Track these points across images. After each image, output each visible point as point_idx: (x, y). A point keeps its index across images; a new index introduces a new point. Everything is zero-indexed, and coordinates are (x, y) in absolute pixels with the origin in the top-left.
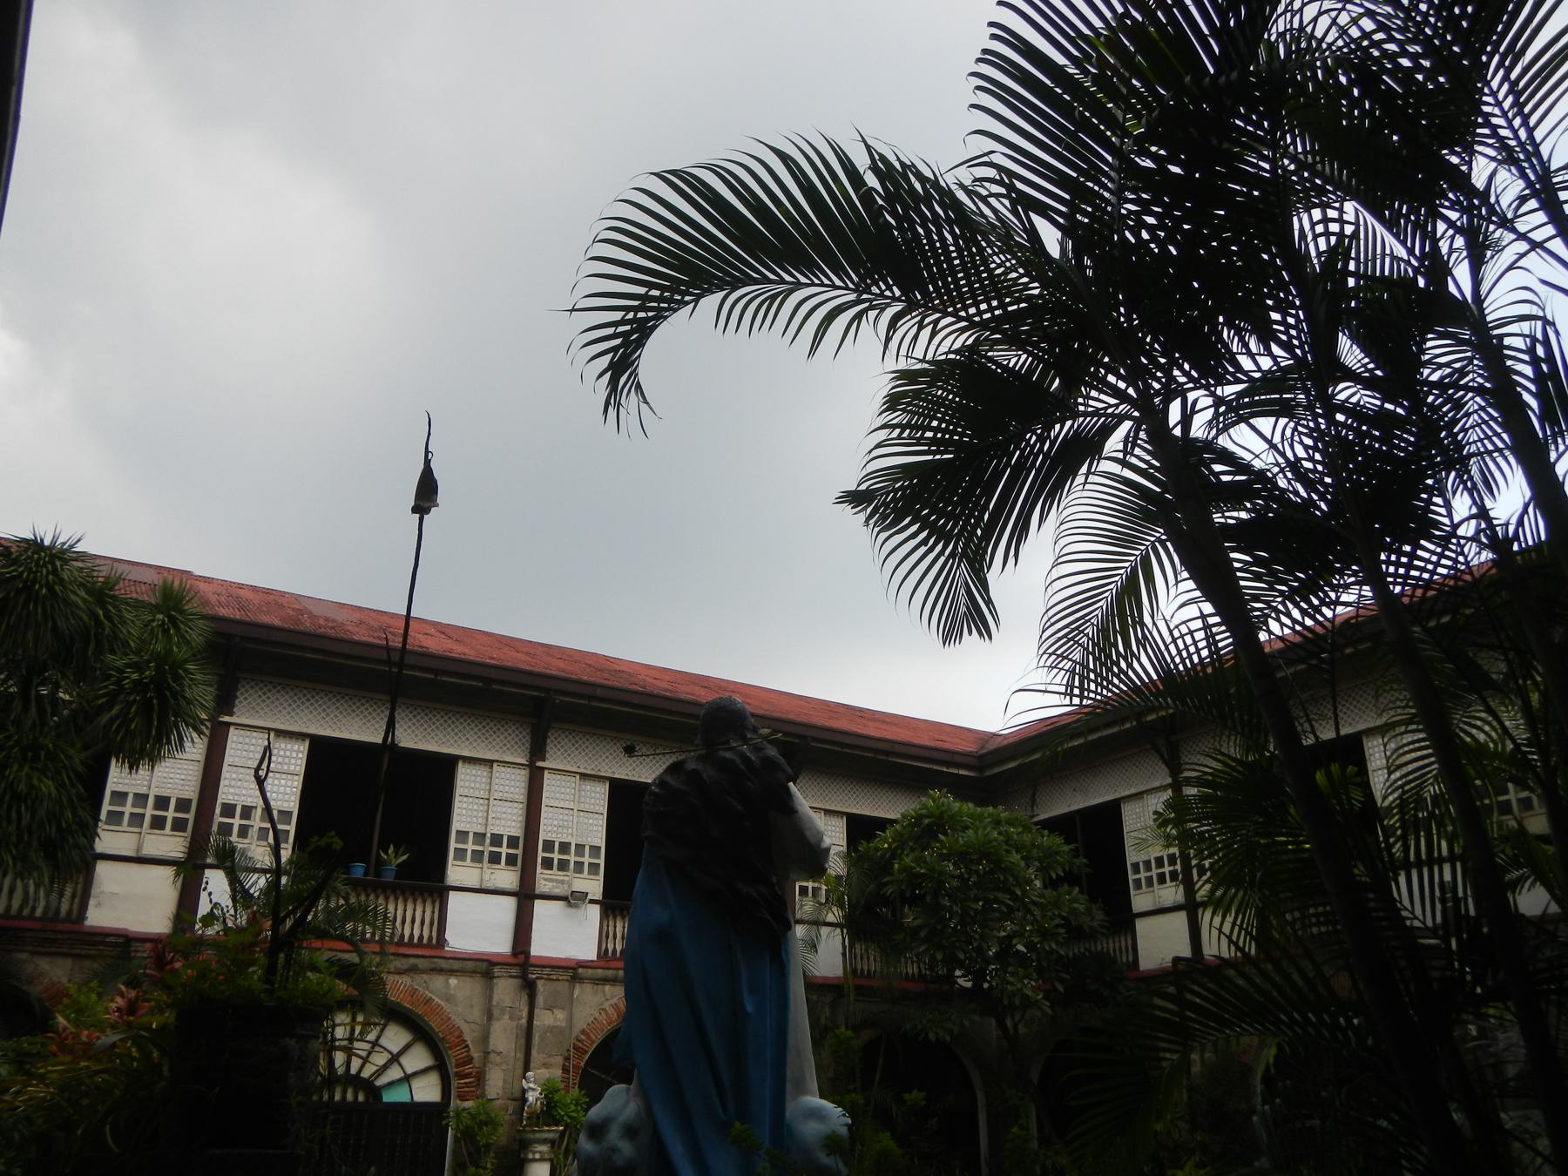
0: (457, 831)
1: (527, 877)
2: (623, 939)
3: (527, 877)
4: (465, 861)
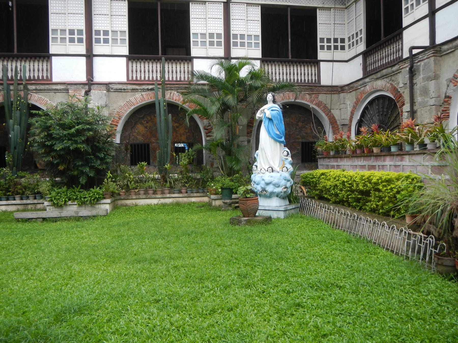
0: (52, 30)
1: (89, 48)
2: (160, 72)
3: (89, 48)
4: (214, 46)
